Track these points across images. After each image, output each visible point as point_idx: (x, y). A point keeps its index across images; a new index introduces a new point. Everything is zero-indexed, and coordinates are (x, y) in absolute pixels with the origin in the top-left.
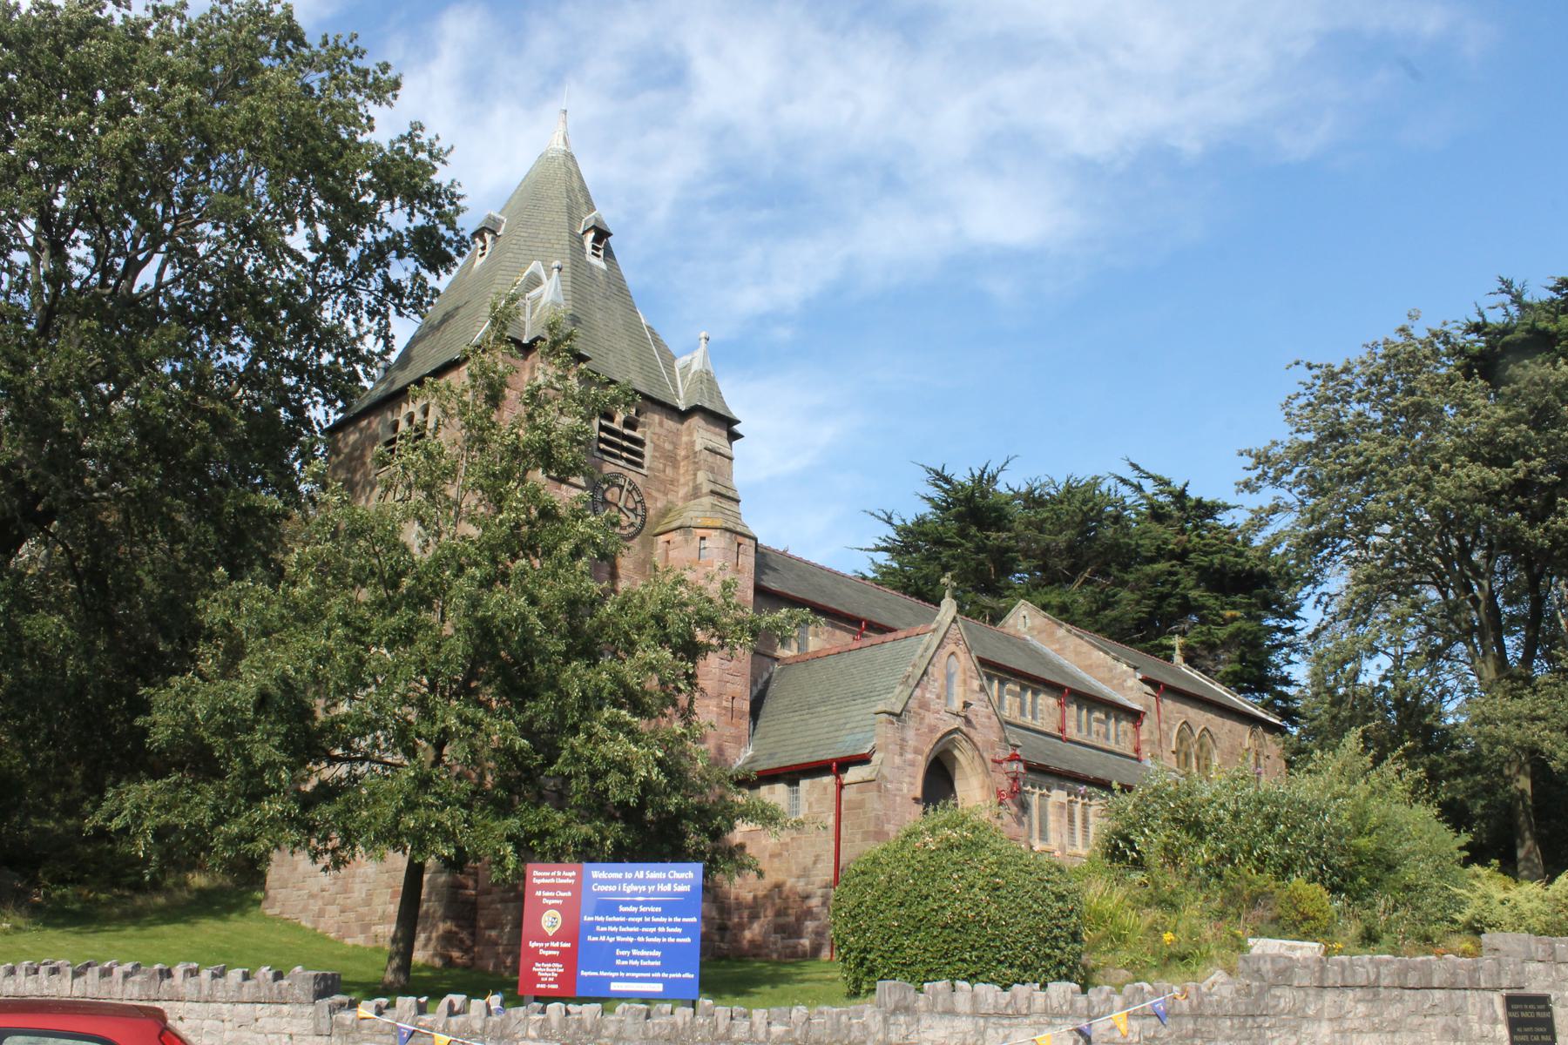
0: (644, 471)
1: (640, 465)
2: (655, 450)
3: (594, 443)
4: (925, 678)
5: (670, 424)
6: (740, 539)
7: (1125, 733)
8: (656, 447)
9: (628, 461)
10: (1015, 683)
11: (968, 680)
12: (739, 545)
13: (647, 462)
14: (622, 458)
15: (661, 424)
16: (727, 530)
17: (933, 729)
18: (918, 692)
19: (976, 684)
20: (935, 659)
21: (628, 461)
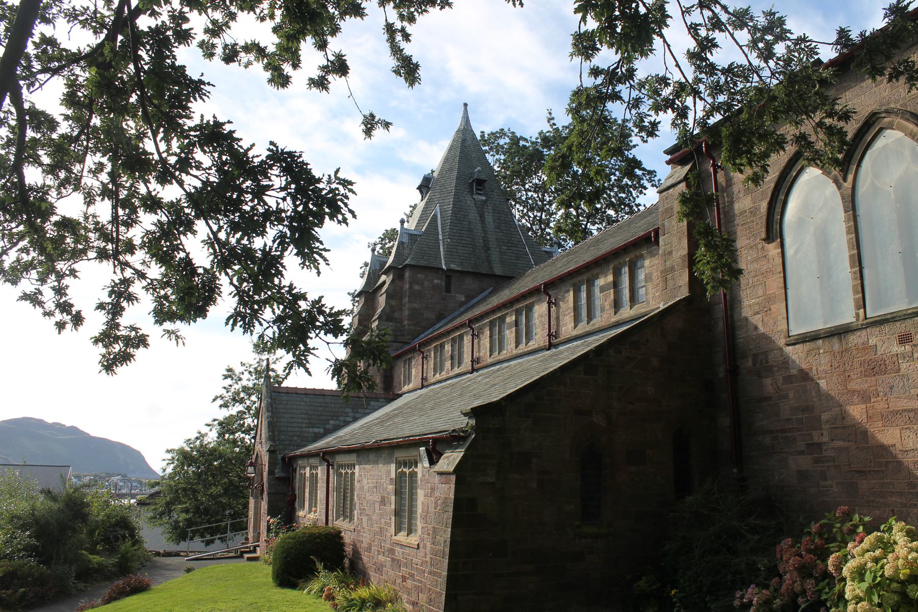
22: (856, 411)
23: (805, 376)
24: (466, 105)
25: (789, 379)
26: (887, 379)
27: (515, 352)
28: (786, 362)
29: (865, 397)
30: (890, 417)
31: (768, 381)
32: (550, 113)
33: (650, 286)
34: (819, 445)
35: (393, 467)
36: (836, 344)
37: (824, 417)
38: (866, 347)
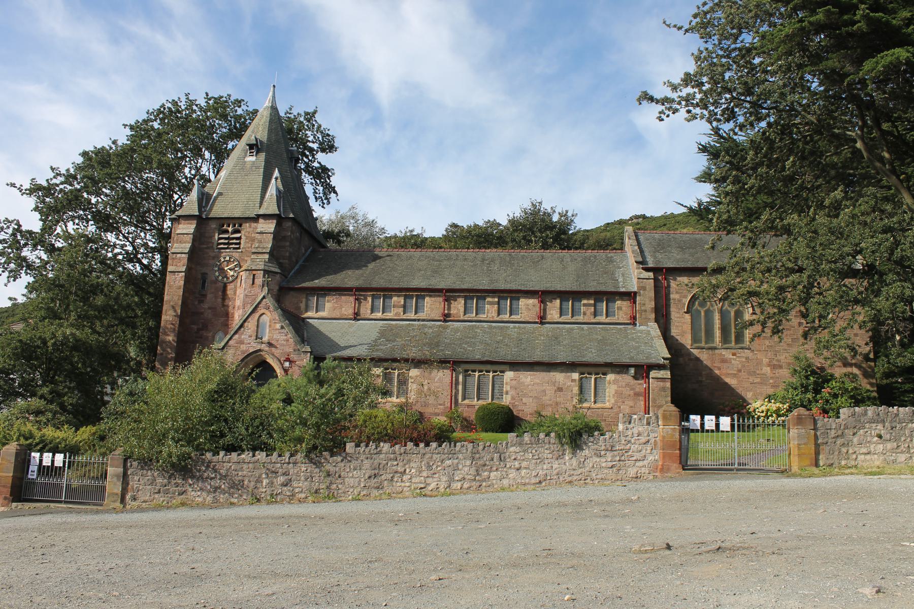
0: (240, 250)
1: (239, 248)
2: (246, 239)
3: (215, 247)
4: (242, 329)
5: (254, 225)
6: (254, 272)
7: (620, 308)
8: (247, 238)
9: (234, 248)
10: (493, 297)
11: (273, 325)
12: (254, 275)
13: (242, 246)
14: (230, 248)
15: (250, 227)
16: (246, 270)
17: (243, 352)
18: (236, 336)
19: (278, 326)
20: (250, 319)
21: (234, 248)
22: (717, 372)
23: (698, 359)
24: (274, 86)
25: (691, 360)
26: (728, 365)
27: (496, 319)
28: (690, 354)
29: (719, 369)
30: (728, 375)
31: (681, 359)
32: (291, 109)
33: (621, 313)
34: (701, 381)
35: (578, 374)
36: (710, 352)
37: (704, 373)
38: (721, 354)
